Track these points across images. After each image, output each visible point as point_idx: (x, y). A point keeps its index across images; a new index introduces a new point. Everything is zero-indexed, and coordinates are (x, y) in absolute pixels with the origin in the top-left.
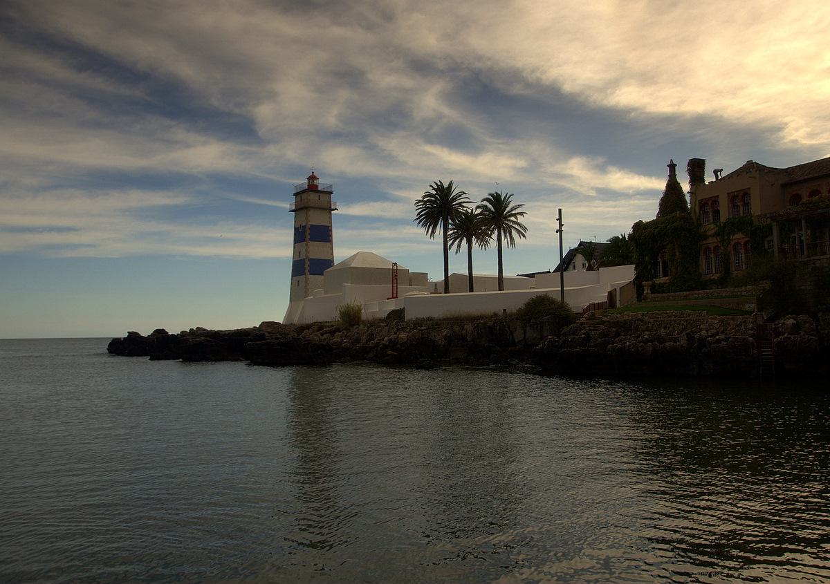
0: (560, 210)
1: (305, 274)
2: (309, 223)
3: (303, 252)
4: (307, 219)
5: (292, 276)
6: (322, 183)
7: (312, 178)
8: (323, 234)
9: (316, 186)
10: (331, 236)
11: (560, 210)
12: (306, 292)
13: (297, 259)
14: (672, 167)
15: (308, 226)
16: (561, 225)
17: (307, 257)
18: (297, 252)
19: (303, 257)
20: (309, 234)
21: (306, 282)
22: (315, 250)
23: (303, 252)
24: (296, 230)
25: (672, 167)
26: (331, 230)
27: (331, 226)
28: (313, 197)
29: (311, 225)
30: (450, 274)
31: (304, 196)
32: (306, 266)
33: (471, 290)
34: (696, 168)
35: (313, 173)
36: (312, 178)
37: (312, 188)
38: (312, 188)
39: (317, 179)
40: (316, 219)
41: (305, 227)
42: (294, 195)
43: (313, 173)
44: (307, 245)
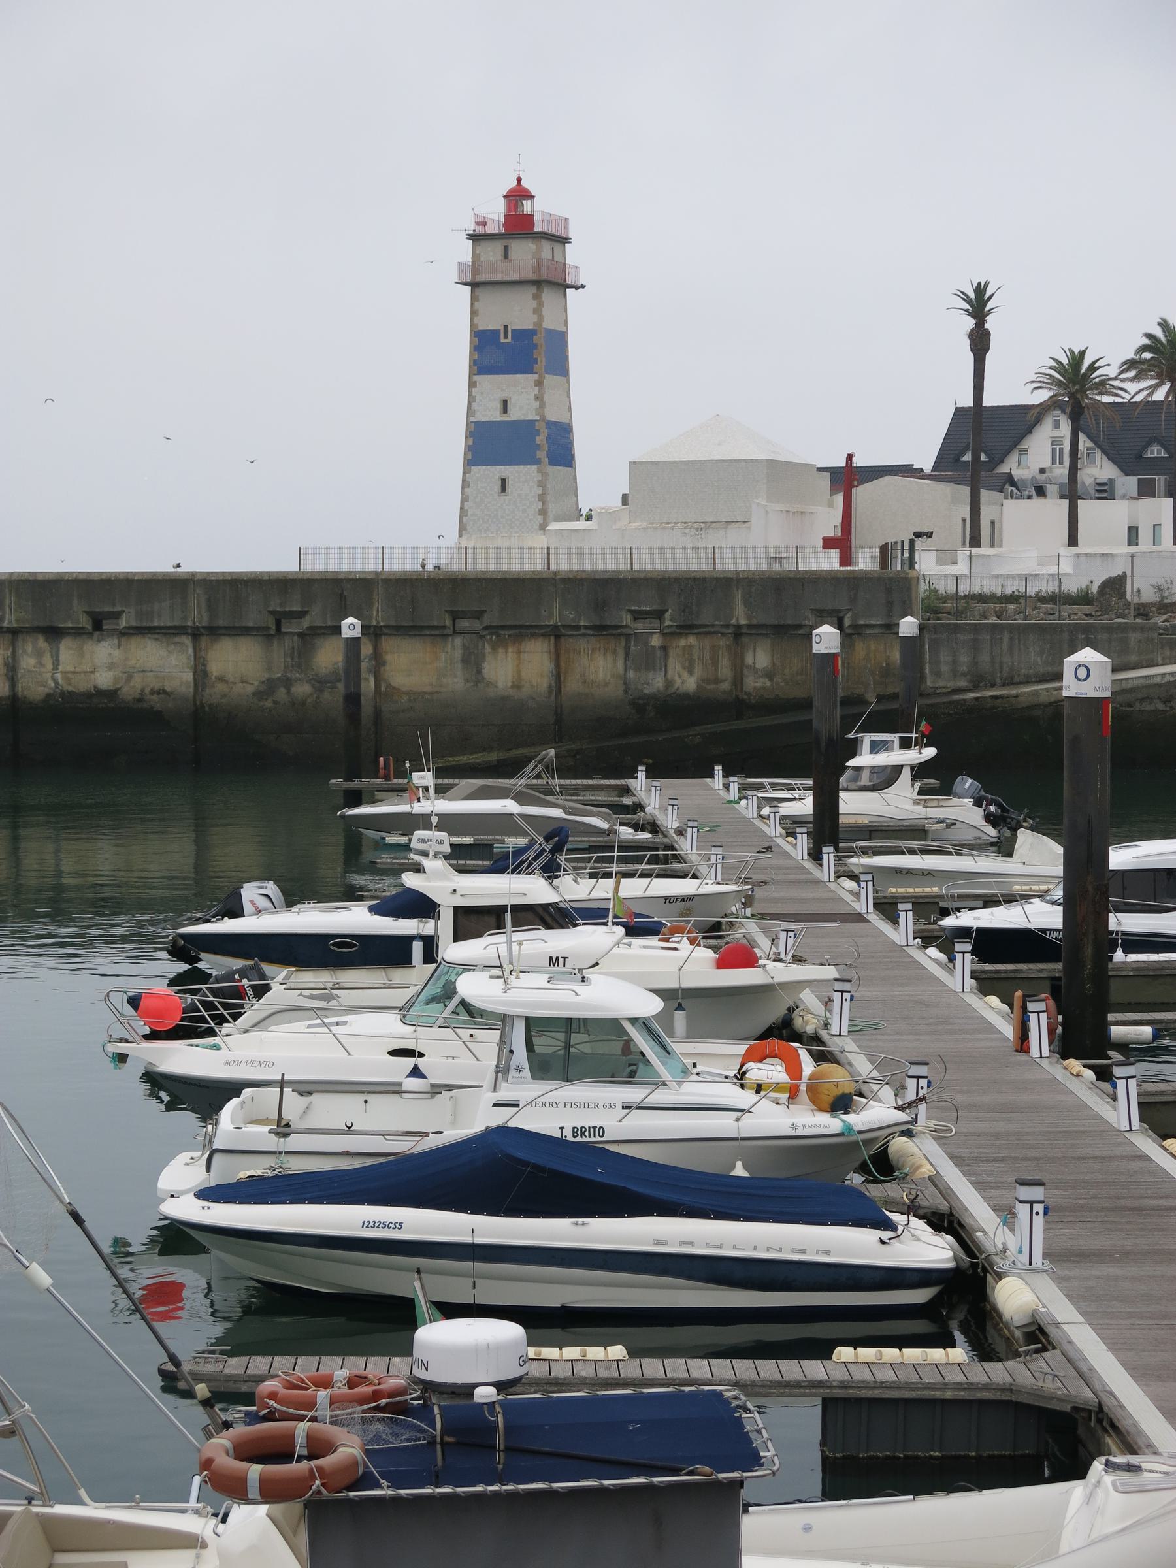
1: (537, 462)
4: (538, 311)
10: (566, 358)
12: (543, 512)
13: (490, 412)
17: (543, 417)
21: (541, 484)
27: (567, 332)
35: (519, 180)
39: (531, 197)
42: (475, 238)
43: (519, 180)
44: (539, 383)
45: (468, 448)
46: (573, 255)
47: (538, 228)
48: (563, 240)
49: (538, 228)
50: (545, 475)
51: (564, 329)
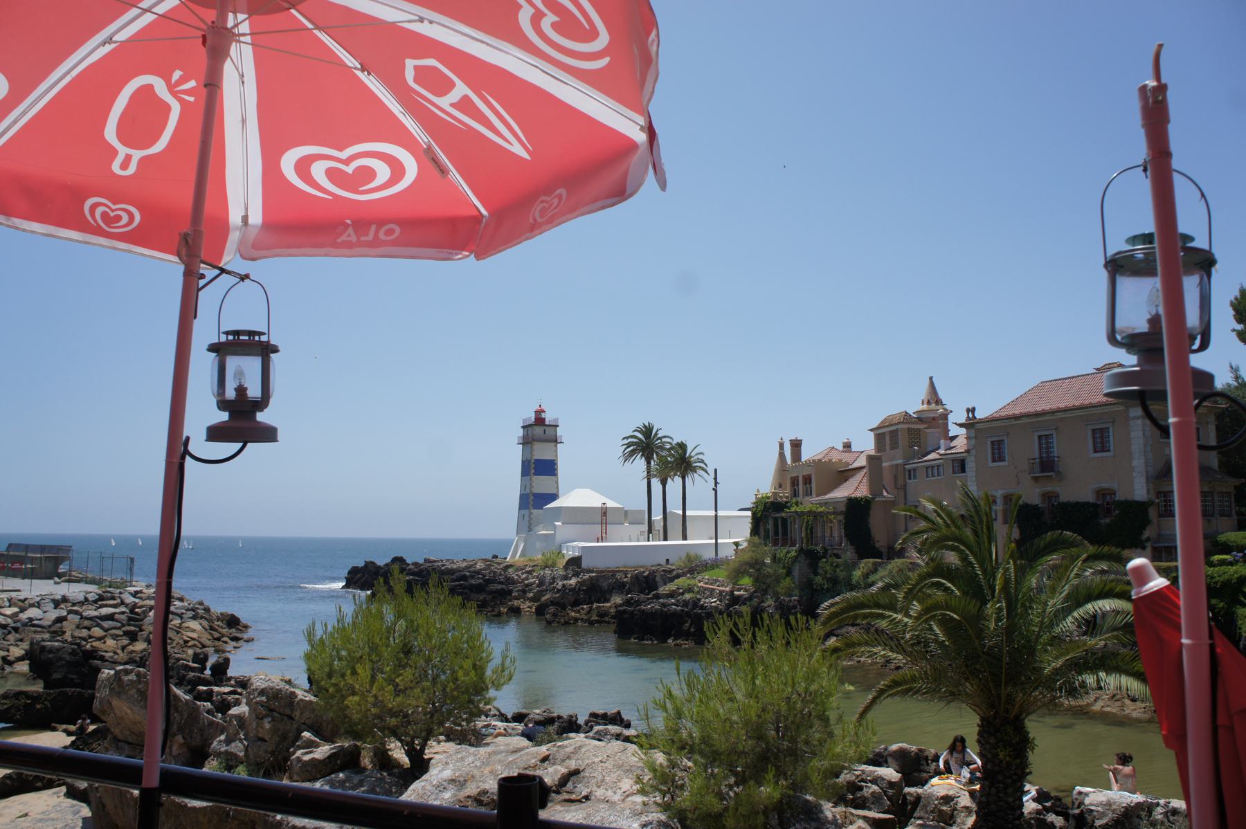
0: (716, 470)
1: (528, 508)
2: (534, 458)
3: (528, 486)
5: (519, 509)
6: (549, 417)
7: (539, 412)
8: (548, 468)
9: (544, 420)
10: (556, 469)
11: (716, 470)
14: (781, 446)
15: (533, 461)
16: (716, 483)
17: (531, 492)
18: (523, 487)
19: (528, 491)
20: (534, 468)
22: (541, 484)
23: (528, 486)
24: (523, 462)
25: (781, 446)
26: (556, 464)
27: (557, 460)
28: (538, 430)
29: (537, 461)
30: (668, 511)
31: (530, 429)
32: (530, 500)
33: (665, 539)
34: (796, 445)
35: (540, 406)
36: (539, 412)
37: (539, 421)
38: (539, 421)
39: (544, 411)
40: (541, 452)
41: (529, 461)
42: (523, 427)
43: (540, 406)
44: (531, 479)
45: (520, 504)
46: (560, 431)
47: (547, 423)
48: (557, 426)
49: (547, 423)
50: (531, 513)
51: (555, 458)
